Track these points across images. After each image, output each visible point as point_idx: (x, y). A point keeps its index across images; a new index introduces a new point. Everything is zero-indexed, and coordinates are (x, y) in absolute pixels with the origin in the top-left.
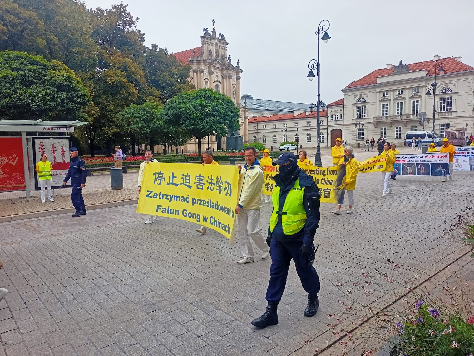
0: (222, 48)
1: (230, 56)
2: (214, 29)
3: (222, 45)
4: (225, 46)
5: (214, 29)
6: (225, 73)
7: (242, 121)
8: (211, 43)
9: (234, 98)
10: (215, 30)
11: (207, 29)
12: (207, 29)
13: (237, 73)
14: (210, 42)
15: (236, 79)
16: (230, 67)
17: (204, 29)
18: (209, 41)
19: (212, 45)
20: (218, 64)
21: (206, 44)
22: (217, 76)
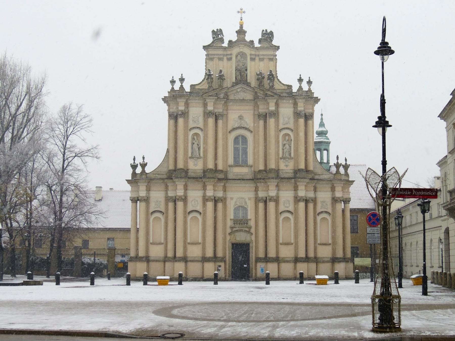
0: (261, 60)
2: (241, 26)
4: (270, 52)
5: (241, 26)
6: (262, 109)
8: (226, 55)
10: (244, 28)
13: (295, 104)
14: (225, 53)
17: (213, 31)
18: (220, 52)
19: (230, 59)
20: (246, 92)
21: (212, 59)
22: (241, 118)
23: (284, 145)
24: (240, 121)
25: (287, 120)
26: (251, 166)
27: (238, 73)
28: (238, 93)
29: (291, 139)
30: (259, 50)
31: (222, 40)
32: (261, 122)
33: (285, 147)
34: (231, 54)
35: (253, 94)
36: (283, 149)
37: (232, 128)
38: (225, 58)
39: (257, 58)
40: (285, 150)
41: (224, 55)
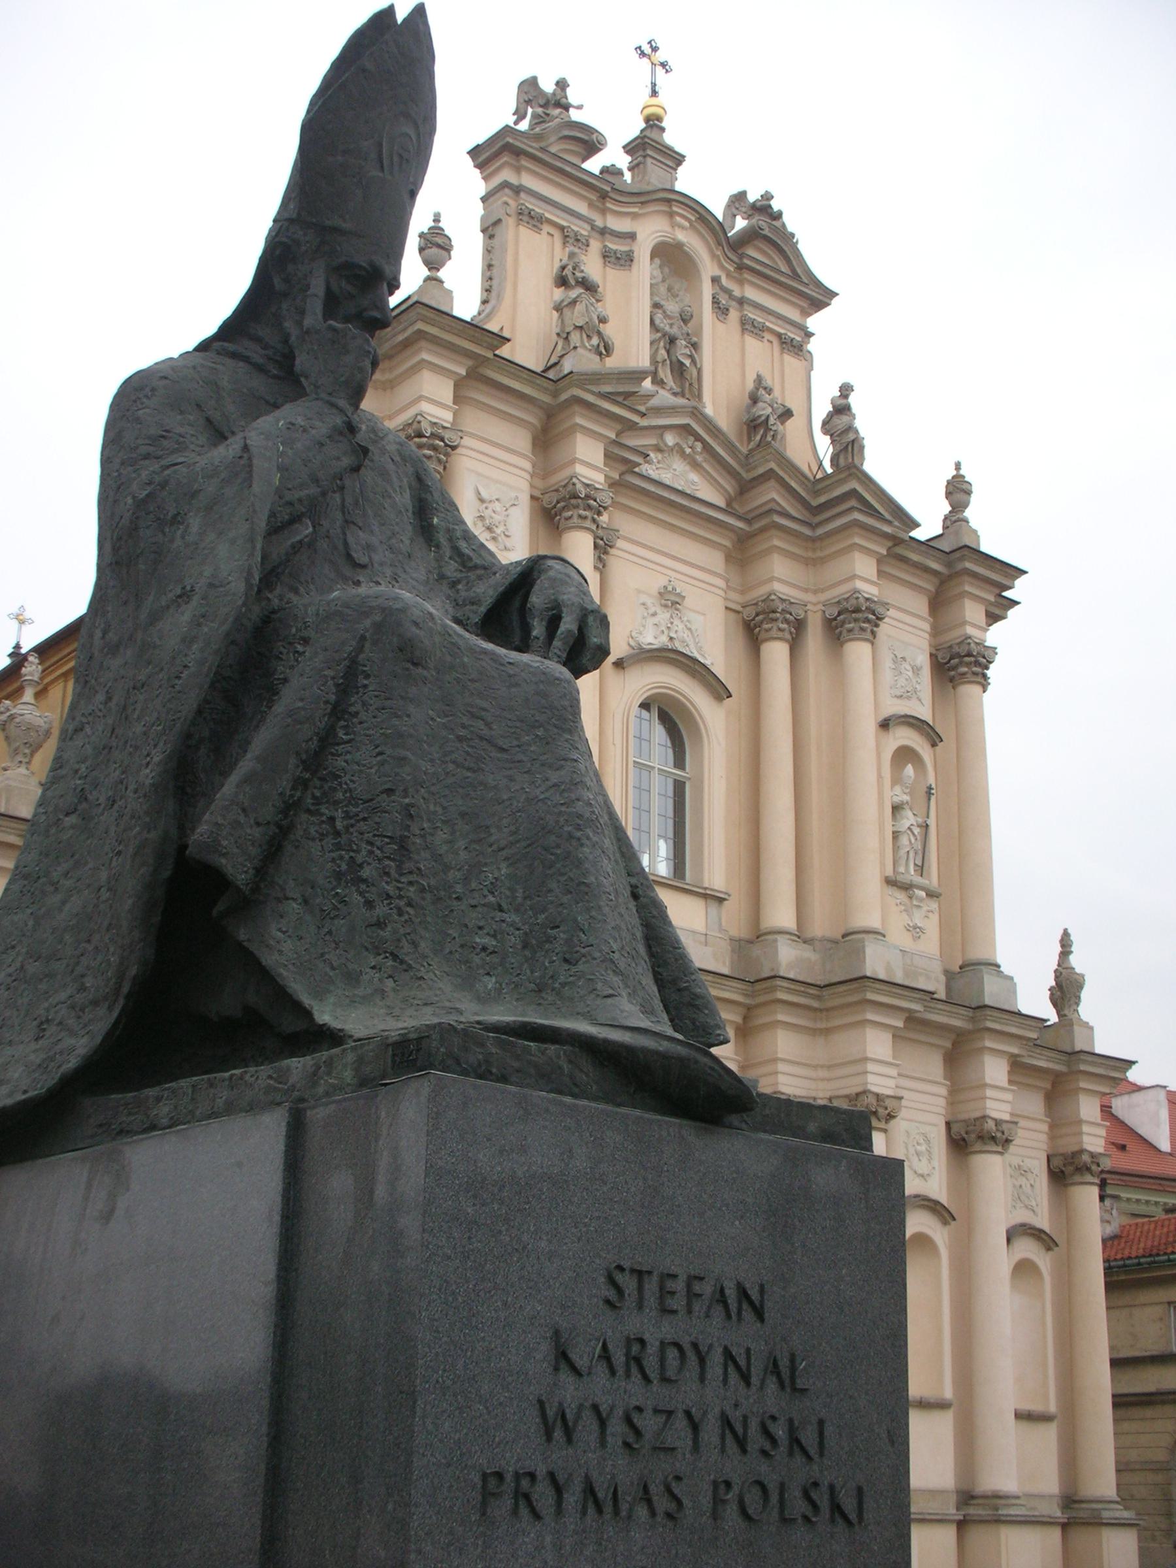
0: (749, 327)
1: (846, 390)
2: (653, 122)
3: (751, 293)
4: (793, 314)
5: (653, 122)
7: (1022, 1216)
8: (603, 232)
9: (907, 887)
11: (562, 85)
12: (562, 85)
13: (939, 603)
15: (923, 659)
16: (853, 503)
18: (581, 208)
19: (625, 260)
20: (695, 465)
23: (896, 809)
24: (668, 615)
25: (910, 674)
26: (721, 900)
27: (663, 353)
28: (660, 456)
29: (930, 788)
30: (747, 275)
31: (590, 143)
32: (776, 653)
33: (905, 823)
34: (632, 236)
35: (730, 486)
36: (896, 835)
37: (633, 643)
38: (595, 245)
39: (734, 315)
40: (904, 840)
41: (593, 227)
